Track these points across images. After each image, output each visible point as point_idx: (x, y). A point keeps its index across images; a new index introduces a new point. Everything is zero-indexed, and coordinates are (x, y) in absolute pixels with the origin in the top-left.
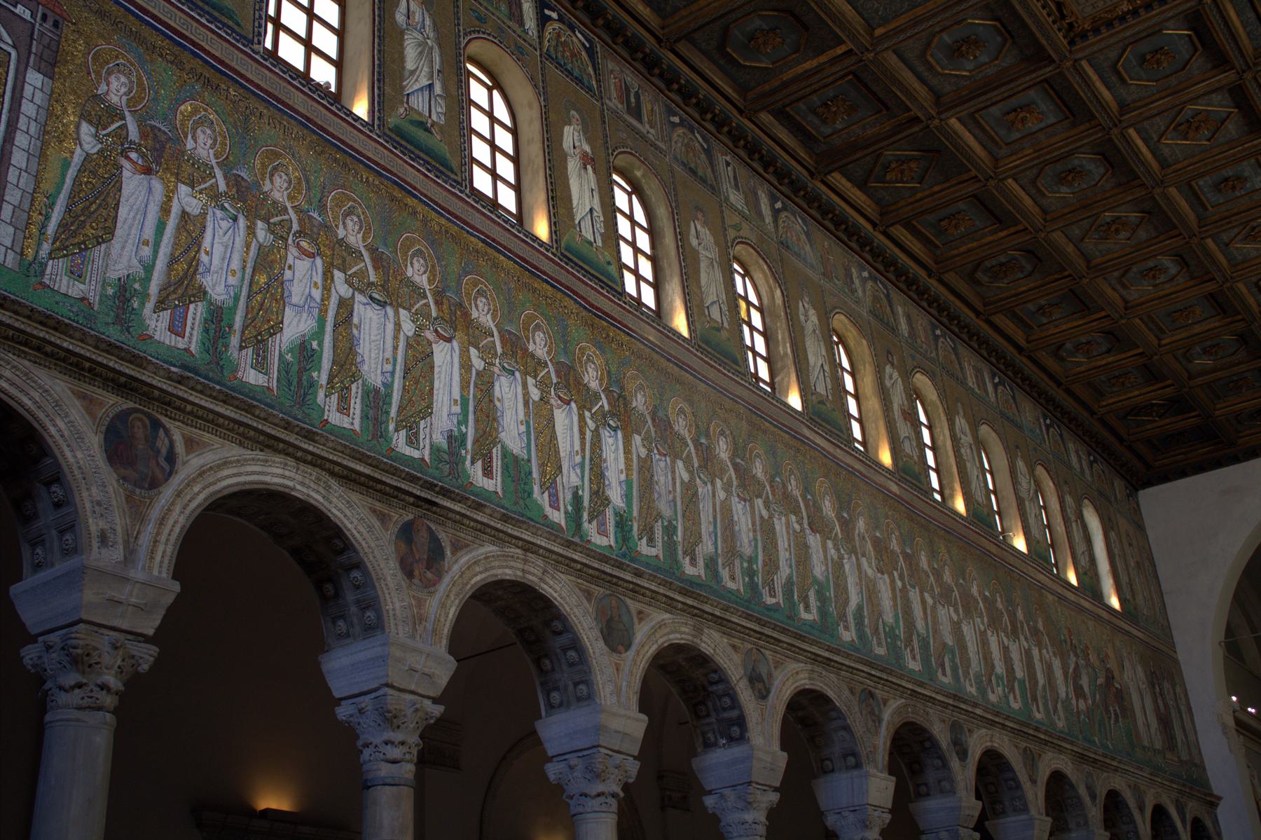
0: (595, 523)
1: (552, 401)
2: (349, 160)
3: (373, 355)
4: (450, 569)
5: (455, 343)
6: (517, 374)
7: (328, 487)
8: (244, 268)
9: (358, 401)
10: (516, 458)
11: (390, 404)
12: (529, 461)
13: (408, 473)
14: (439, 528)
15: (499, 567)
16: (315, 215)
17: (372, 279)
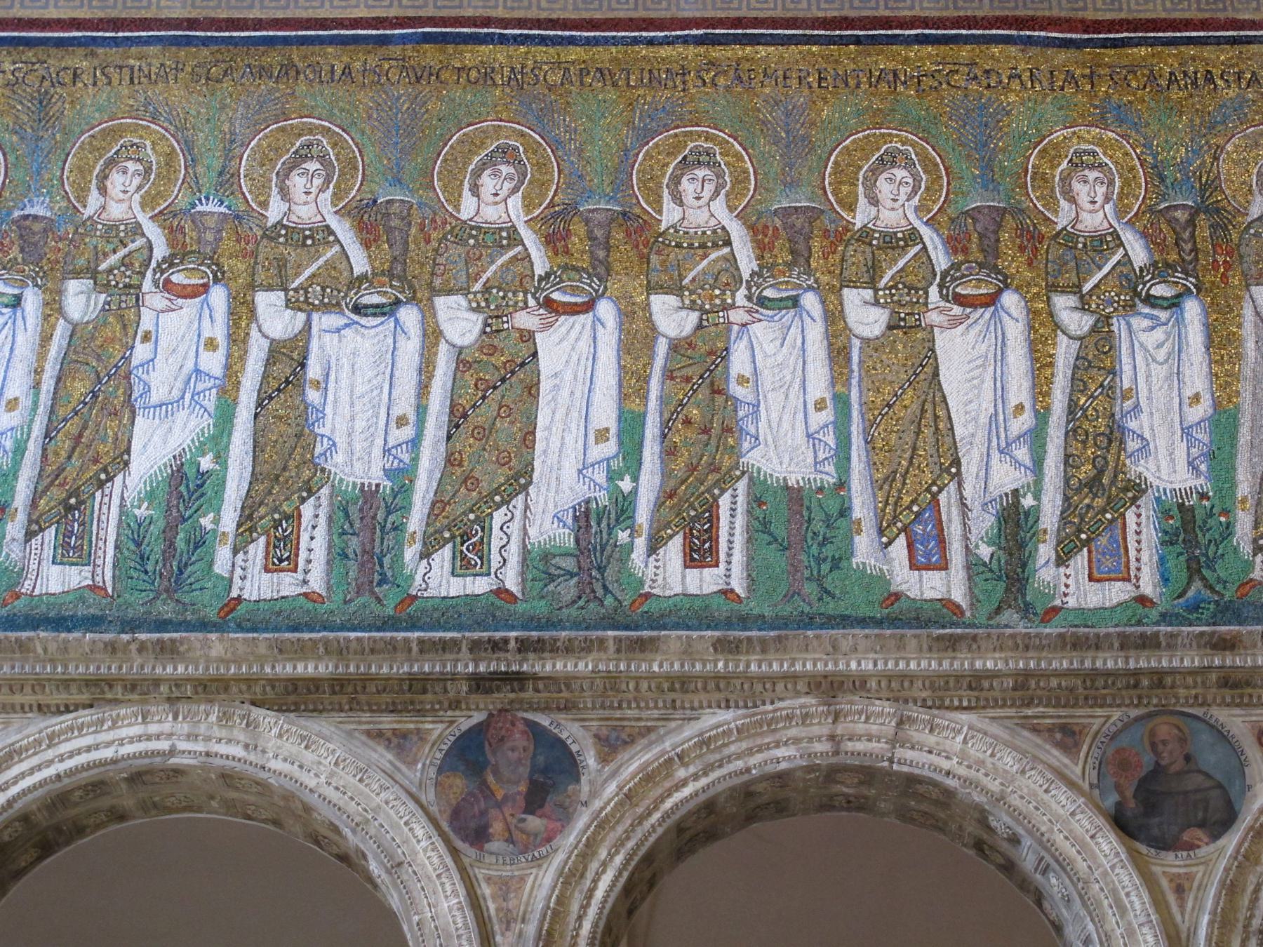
0: (1081, 560)
1: (933, 317)
2: (295, 54)
3: (360, 425)
4: (594, 794)
5: (605, 309)
6: (810, 301)
7: (251, 725)
8: (37, 386)
9: (321, 532)
10: (795, 496)
11: (406, 509)
12: (842, 485)
13: (421, 642)
14: (561, 717)
15: (750, 752)
16: (212, 207)
17: (357, 271)
